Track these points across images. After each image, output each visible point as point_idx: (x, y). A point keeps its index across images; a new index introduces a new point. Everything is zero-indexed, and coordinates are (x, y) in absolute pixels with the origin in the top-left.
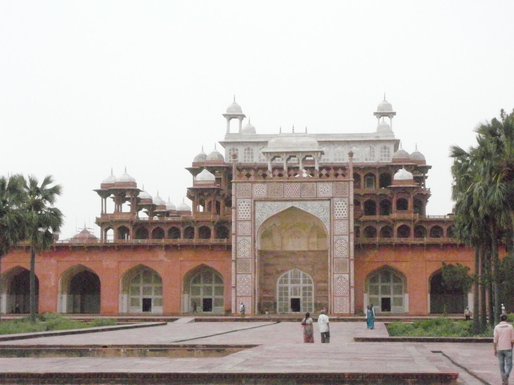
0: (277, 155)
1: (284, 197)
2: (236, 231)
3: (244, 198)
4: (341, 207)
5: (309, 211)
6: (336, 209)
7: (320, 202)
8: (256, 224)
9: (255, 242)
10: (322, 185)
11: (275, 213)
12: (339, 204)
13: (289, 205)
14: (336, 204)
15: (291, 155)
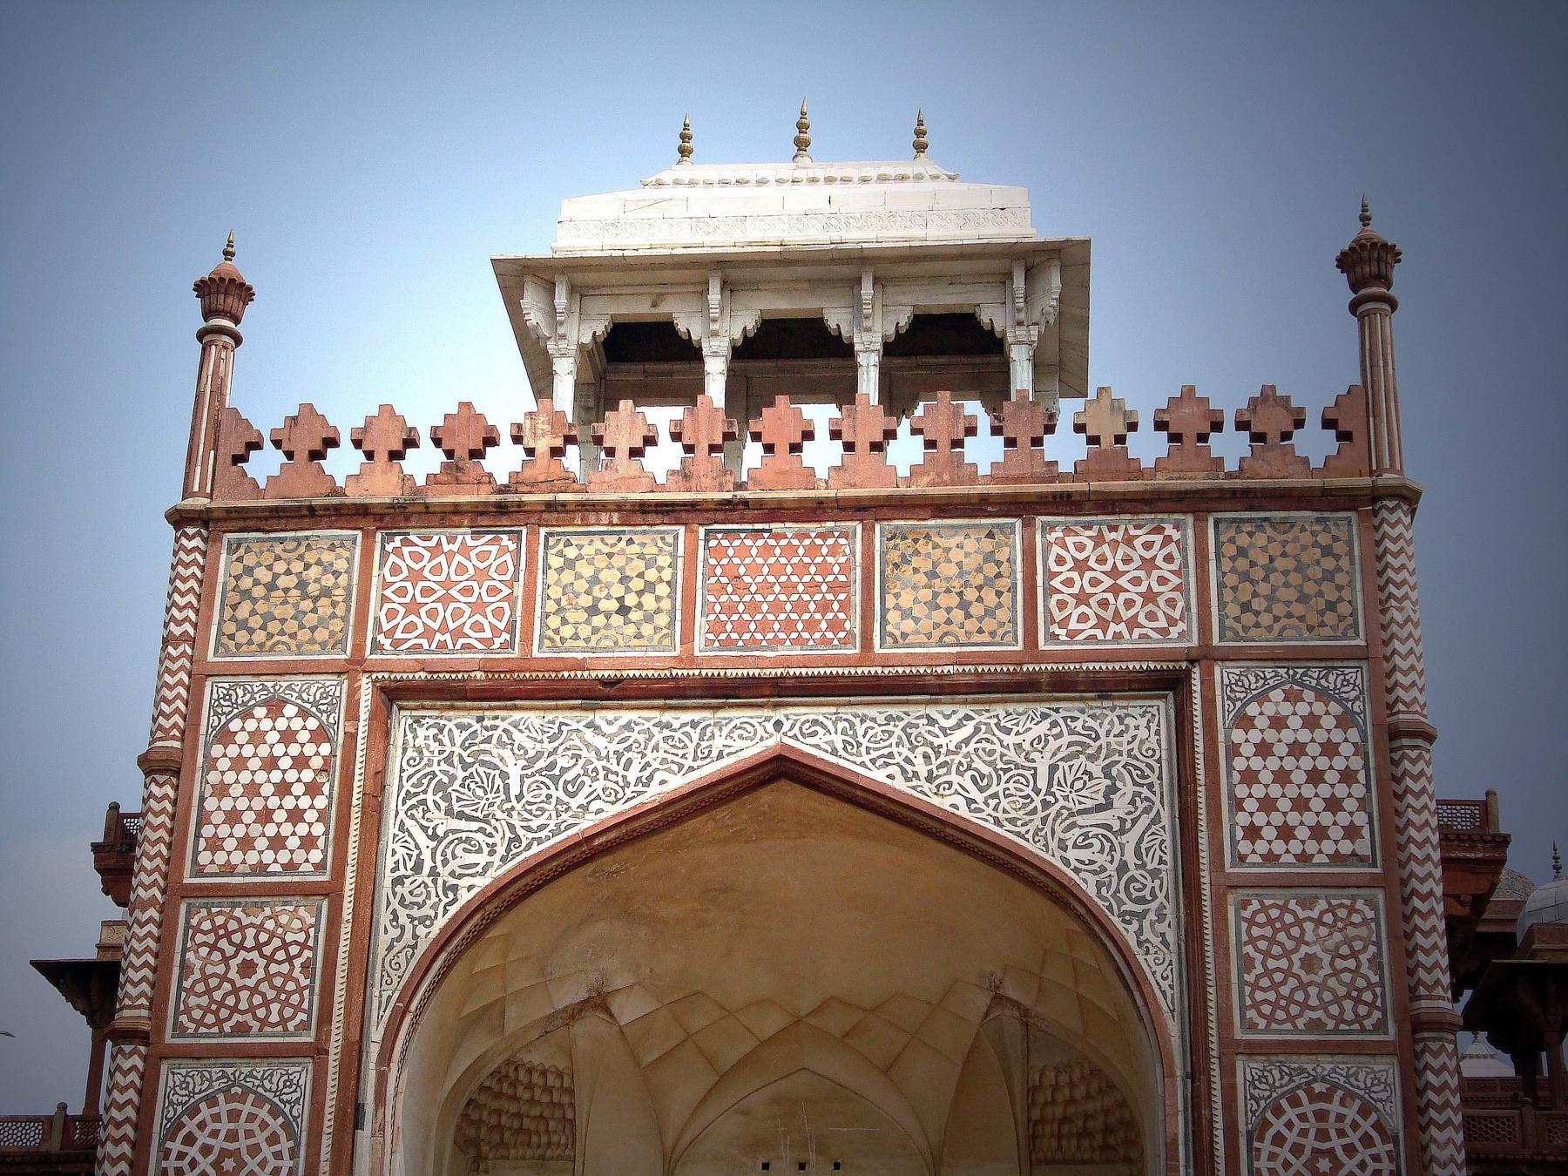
0: (638, 308)
1: (690, 660)
2: (157, 1004)
3: (282, 671)
4: (1297, 749)
5: (944, 803)
6: (1250, 777)
7: (1080, 715)
8: (383, 940)
9: (352, 1116)
10: (1085, 537)
11: (587, 823)
12: (1278, 723)
13: (741, 738)
14: (1245, 722)
15: (784, 305)
